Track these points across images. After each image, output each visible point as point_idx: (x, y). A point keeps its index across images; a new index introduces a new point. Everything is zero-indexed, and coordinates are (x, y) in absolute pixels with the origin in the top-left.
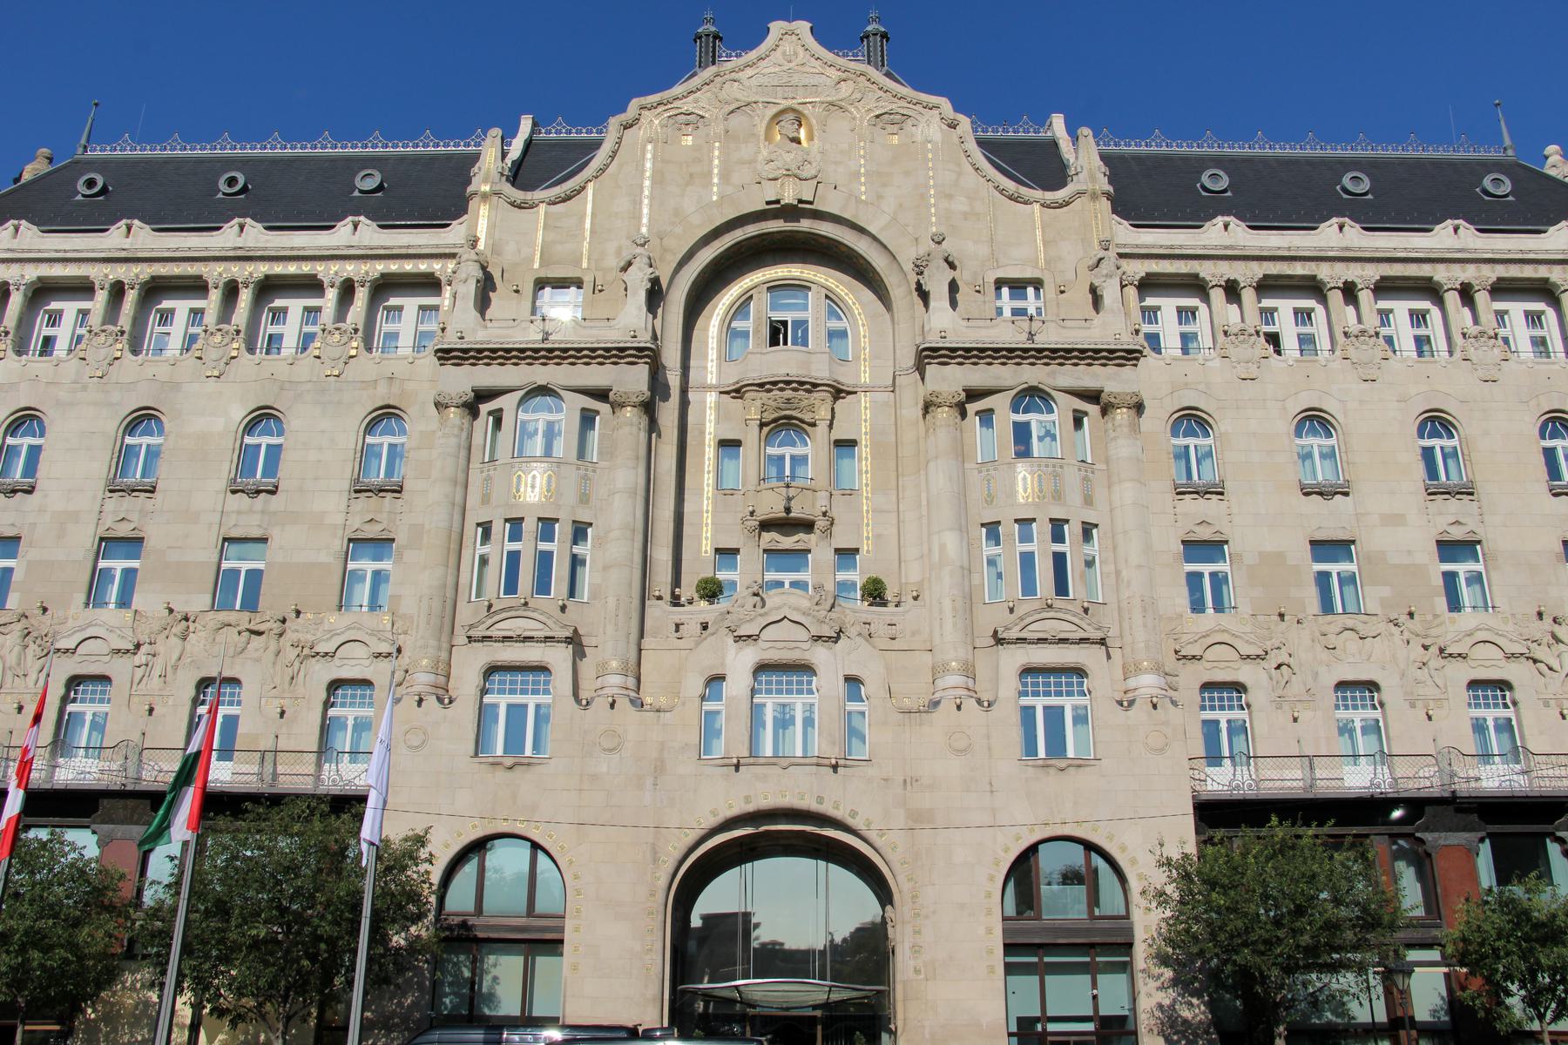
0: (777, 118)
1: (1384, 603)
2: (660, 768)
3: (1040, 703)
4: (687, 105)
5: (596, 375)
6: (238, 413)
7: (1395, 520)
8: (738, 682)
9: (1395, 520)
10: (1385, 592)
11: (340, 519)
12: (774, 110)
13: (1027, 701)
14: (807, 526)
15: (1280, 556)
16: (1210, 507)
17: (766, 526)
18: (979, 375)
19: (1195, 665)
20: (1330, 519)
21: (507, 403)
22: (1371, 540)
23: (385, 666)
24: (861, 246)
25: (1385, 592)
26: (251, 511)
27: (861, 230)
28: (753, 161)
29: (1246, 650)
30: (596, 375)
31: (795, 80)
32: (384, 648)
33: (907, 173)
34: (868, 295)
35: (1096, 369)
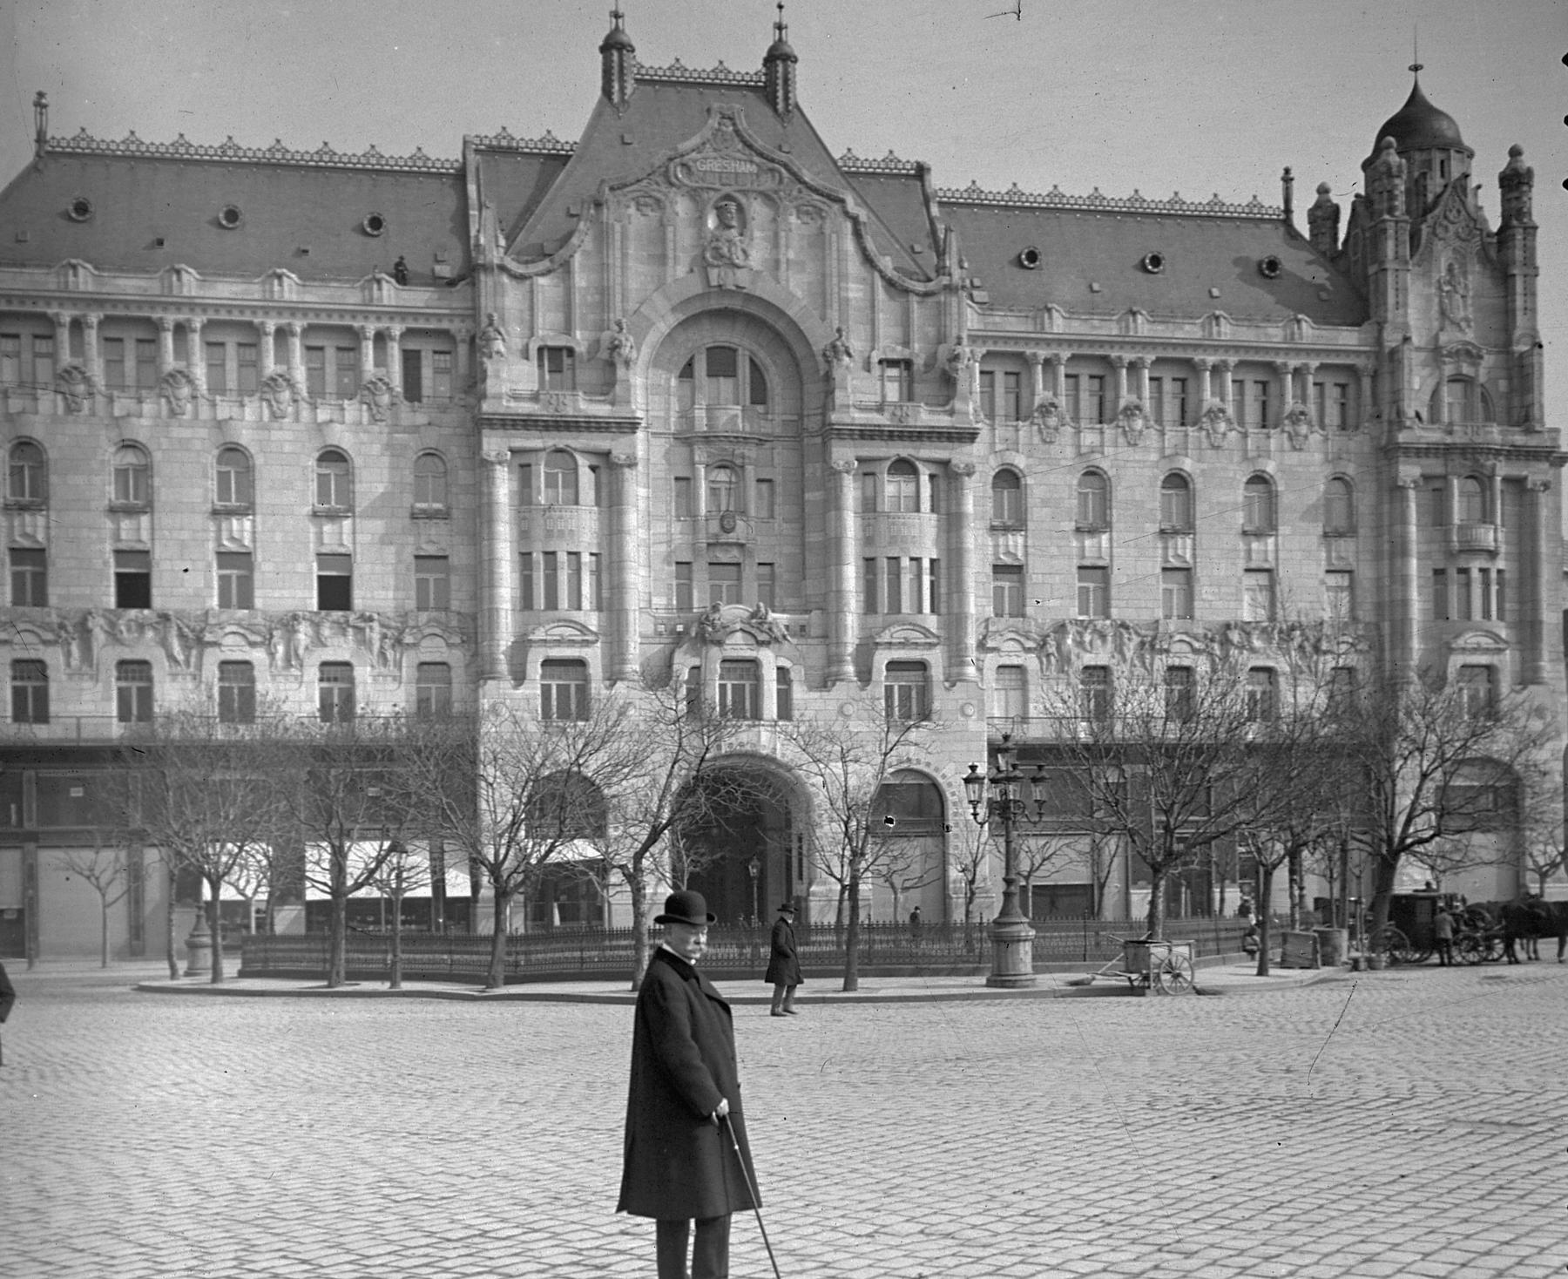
12: (714, 196)
16: (1015, 541)
24: (780, 326)
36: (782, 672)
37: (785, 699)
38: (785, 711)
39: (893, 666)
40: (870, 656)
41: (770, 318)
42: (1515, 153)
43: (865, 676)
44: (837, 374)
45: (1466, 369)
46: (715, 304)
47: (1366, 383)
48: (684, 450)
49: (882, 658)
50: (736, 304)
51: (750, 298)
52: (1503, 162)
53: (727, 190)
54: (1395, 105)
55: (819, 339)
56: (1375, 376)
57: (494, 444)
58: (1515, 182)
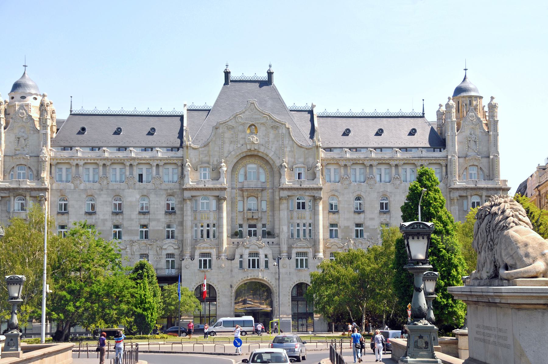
0: (250, 127)
1: (368, 236)
2: (231, 271)
3: (299, 258)
4: (230, 123)
5: (217, 193)
6: (138, 197)
7: (372, 219)
8: (246, 257)
9: (372, 219)
10: (368, 234)
11: (163, 220)
12: (248, 125)
13: (297, 258)
14: (257, 219)
15: (349, 227)
16: (336, 216)
17: (248, 219)
18: (290, 193)
19: (329, 250)
20: (359, 219)
21: (197, 198)
22: (368, 223)
23: (176, 251)
24: (268, 159)
25: (368, 234)
26: (144, 218)
27: (268, 156)
28: (245, 138)
29: (339, 246)
30: (217, 193)
31: (255, 116)
32: (176, 247)
33: (278, 141)
34: (268, 167)
35: (314, 191)
36: (266, 256)
37: (267, 262)
38: (267, 266)
39: (298, 254)
40: (291, 251)
41: (265, 157)
42: (492, 98)
43: (289, 258)
44: (282, 173)
45: (476, 163)
46: (249, 154)
47: (444, 168)
48: (241, 193)
49: (294, 251)
50: (256, 153)
51: (258, 151)
52: (489, 101)
53: (253, 123)
54: (457, 83)
55: (278, 163)
56: (446, 166)
57: (187, 194)
58: (492, 107)
